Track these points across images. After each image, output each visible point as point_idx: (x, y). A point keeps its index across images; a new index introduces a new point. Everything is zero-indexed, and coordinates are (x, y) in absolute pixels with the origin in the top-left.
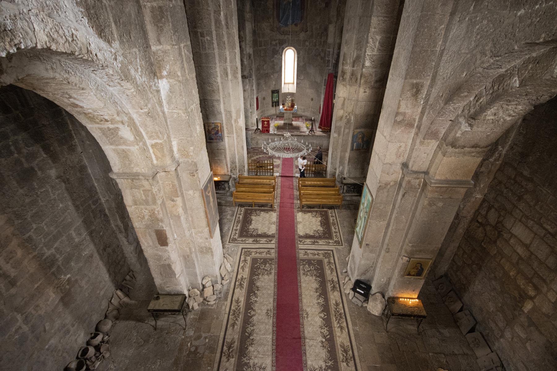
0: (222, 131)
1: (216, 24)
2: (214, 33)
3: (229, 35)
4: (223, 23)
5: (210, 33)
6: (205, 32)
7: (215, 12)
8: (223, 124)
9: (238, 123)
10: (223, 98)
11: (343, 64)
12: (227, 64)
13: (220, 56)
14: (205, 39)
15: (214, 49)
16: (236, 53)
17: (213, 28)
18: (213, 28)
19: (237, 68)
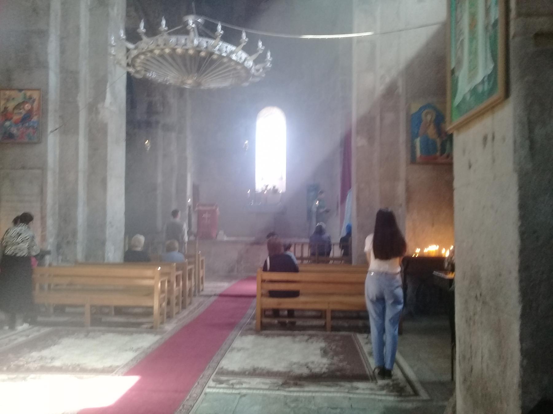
0: (43, 111)
8: (47, 92)
9: (97, 112)
10: (62, 38)
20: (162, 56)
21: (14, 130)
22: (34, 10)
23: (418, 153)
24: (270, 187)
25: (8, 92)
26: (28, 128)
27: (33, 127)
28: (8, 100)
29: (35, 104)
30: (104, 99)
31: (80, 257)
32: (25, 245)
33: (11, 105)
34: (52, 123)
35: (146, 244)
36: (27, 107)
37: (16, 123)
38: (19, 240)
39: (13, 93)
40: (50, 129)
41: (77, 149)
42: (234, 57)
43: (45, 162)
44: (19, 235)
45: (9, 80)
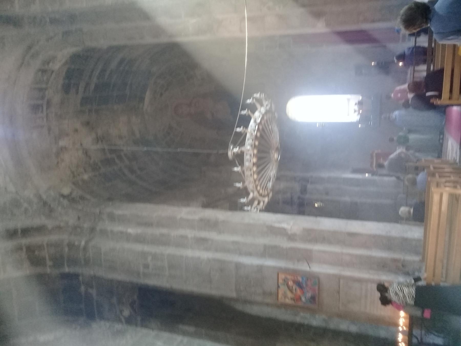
0: (294, 272)
2: (146, 248)
3: (159, 224)
5: (144, 255)
10: (241, 254)
17: (139, 247)
18: (139, 247)
20: (258, 173)
21: (309, 295)
24: (356, 108)
25: (280, 296)
26: (306, 285)
30: (284, 229)
31: (417, 258)
32: (406, 290)
33: (289, 295)
34: (303, 267)
36: (291, 283)
37: (303, 293)
38: (401, 295)
40: (308, 269)
41: (324, 252)
42: (259, 121)
43: (334, 276)
44: (396, 294)
45: (271, 294)
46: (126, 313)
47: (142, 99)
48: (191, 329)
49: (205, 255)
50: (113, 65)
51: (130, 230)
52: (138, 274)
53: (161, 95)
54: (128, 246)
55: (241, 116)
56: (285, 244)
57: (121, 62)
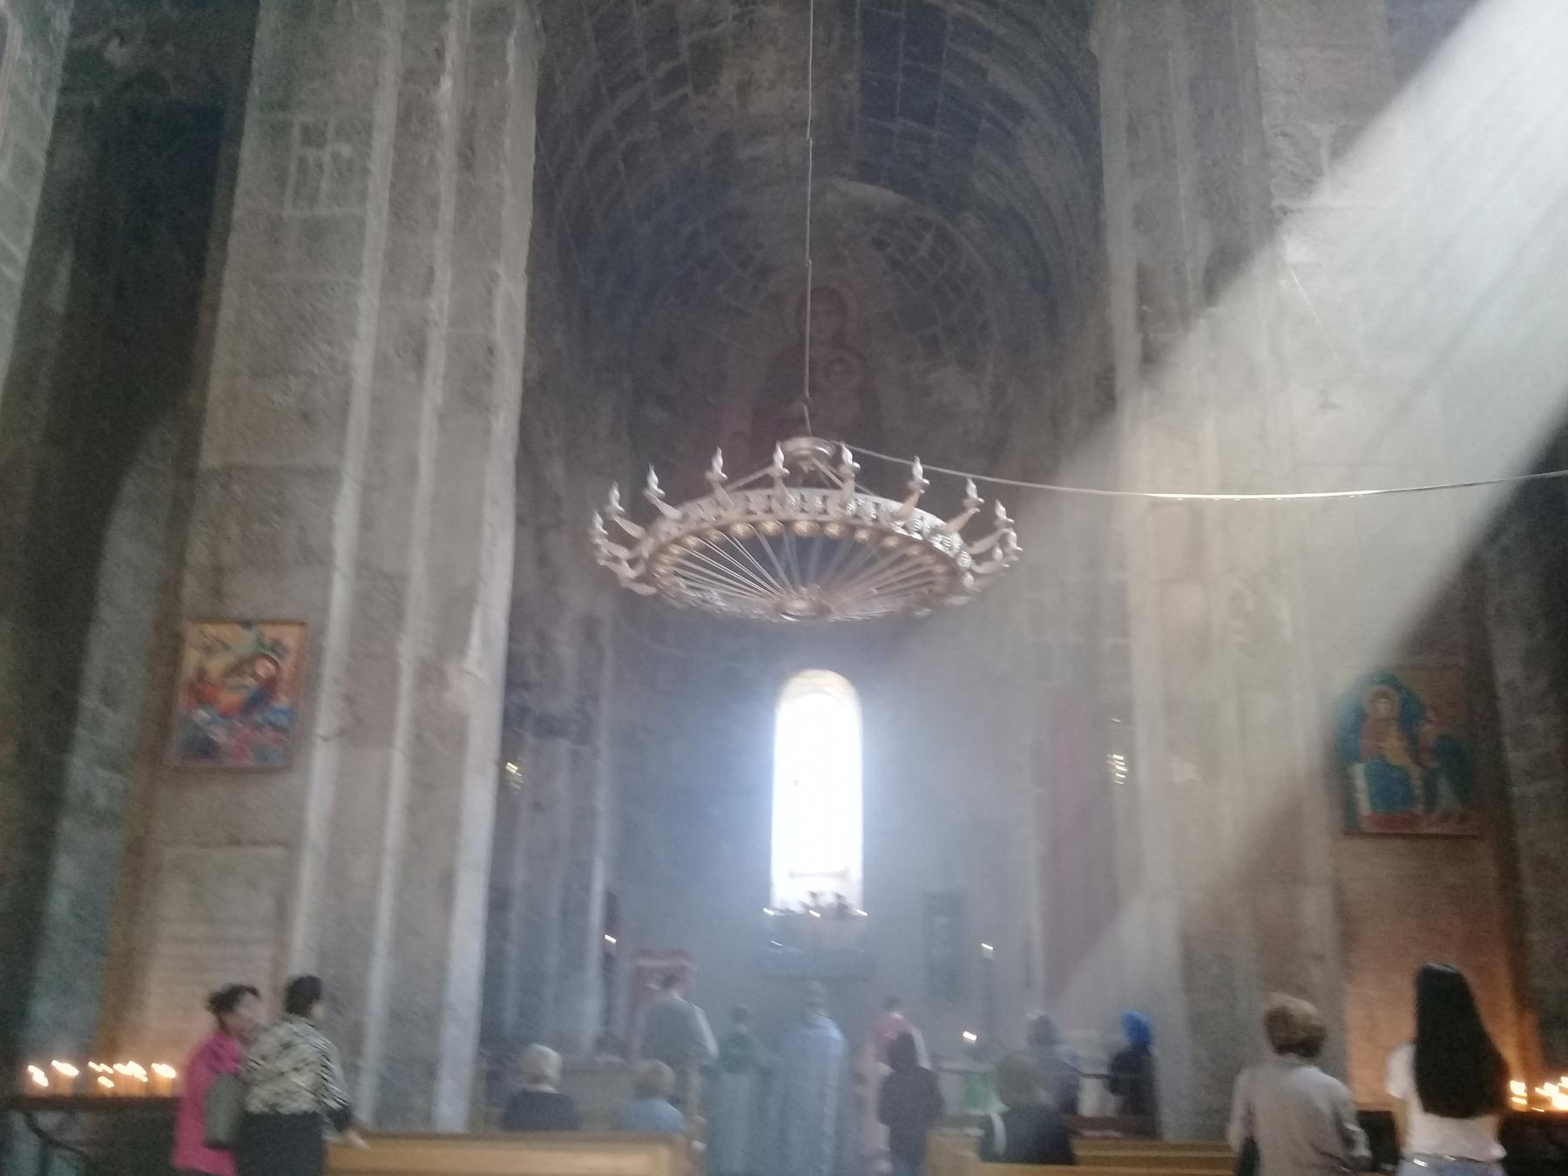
0: (307, 682)
1: (404, 117)
2: (382, 142)
3: (468, 197)
4: (447, 118)
5: (361, 131)
6: (332, 123)
7: (409, 75)
8: (321, 631)
10: (367, 489)
11: (1142, 318)
12: (433, 304)
13: (395, 262)
14: (326, 158)
15: (363, 197)
16: (494, 277)
18: (385, 112)
19: (491, 351)
20: (752, 543)
21: (220, 735)
22: (305, 416)
23: (1364, 806)
24: (828, 899)
25: (211, 630)
26: (258, 727)
27: (276, 728)
28: (208, 650)
29: (287, 665)
30: (462, 648)
33: (216, 665)
34: (327, 717)
35: (565, 1072)
37: (225, 715)
39: (226, 632)
41: (384, 786)
43: (300, 823)
45: (218, 594)
46: (116, 53)
47: (867, 173)
48: (58, 299)
49: (362, 357)
50: (1002, 77)
51: (447, 83)
52: (283, 106)
53: (879, 244)
54: (390, 70)
55: (964, 482)
56: (409, 649)
57: (1014, 109)
